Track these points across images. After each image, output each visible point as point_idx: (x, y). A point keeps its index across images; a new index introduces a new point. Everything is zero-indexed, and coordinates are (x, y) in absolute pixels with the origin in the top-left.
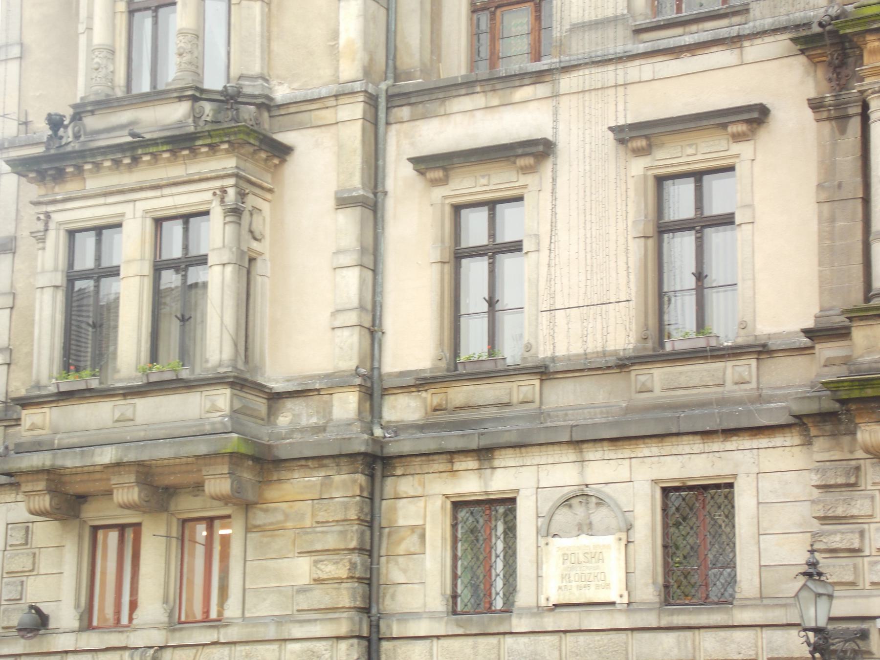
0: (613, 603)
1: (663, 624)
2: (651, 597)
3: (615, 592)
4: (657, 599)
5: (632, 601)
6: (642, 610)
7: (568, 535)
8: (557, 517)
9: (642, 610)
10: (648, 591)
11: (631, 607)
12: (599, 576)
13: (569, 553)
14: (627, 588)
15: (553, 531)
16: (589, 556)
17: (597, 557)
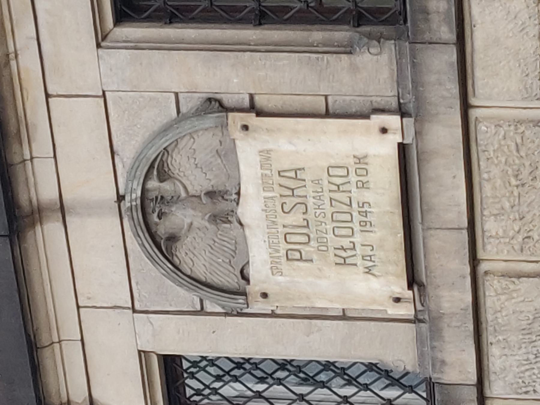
0: (403, 148)
1: (447, 33)
2: (384, 58)
3: (376, 145)
4: (390, 45)
5: (394, 104)
6: (416, 84)
7: (239, 251)
8: (200, 272)
9: (416, 84)
10: (372, 69)
11: (411, 107)
12: (339, 181)
13: (284, 247)
14: (366, 116)
15: (232, 280)
16: (290, 202)
17: (291, 184)
